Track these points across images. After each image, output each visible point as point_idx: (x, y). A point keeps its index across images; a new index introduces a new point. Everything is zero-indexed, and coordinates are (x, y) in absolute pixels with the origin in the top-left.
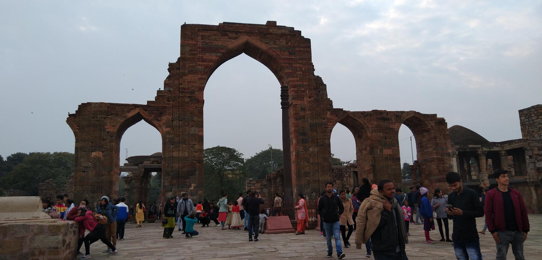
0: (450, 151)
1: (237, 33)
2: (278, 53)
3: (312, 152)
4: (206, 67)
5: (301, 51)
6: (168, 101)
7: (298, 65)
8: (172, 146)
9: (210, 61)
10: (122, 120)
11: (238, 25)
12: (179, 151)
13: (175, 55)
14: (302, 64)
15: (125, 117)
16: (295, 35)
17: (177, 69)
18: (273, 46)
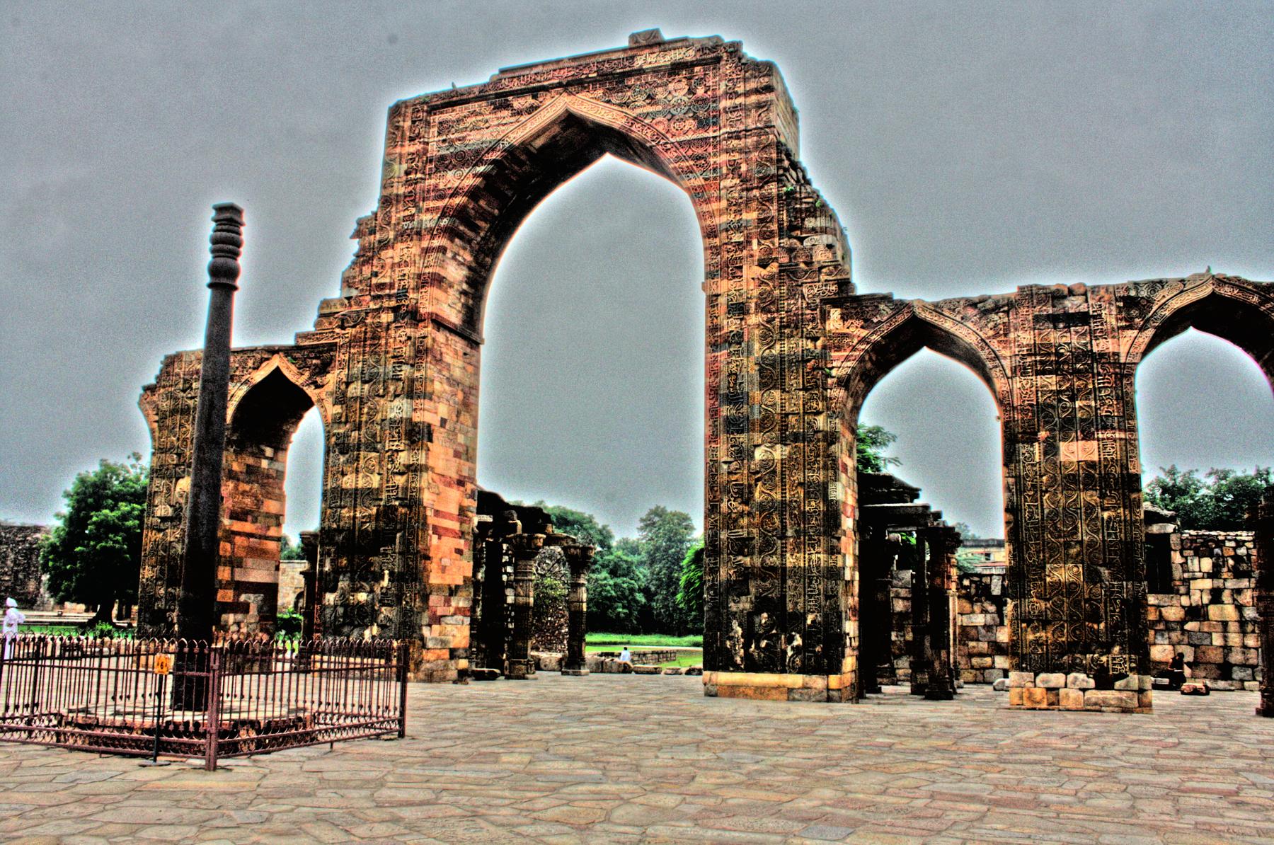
1: (534, 92)
2: (660, 128)
3: (765, 464)
6: (343, 328)
7: (724, 158)
8: (342, 459)
12: (357, 472)
14: (740, 151)
18: (645, 110)
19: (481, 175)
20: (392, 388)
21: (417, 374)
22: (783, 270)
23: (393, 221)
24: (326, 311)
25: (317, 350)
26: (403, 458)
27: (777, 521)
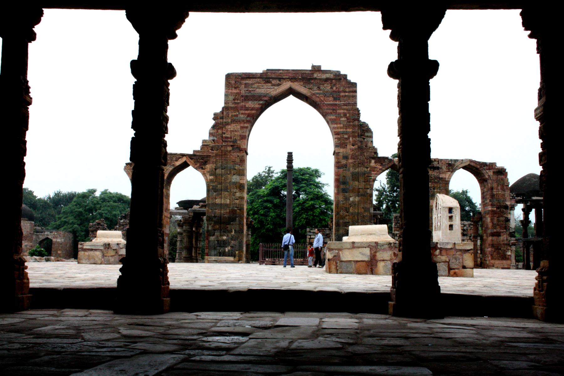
0: (508, 203)
1: (280, 79)
2: (322, 98)
3: (353, 202)
4: (249, 115)
5: (345, 96)
6: (212, 150)
7: (342, 111)
8: (215, 194)
9: (253, 109)
10: (171, 169)
11: (281, 72)
13: (218, 105)
14: (347, 110)
15: (173, 165)
16: (340, 79)
17: (221, 119)
18: (317, 92)
19: (261, 104)
20: (232, 172)
21: (241, 168)
22: (359, 147)
23: (230, 116)
24: (205, 144)
25: (202, 157)
26: (238, 194)
27: (356, 218)
